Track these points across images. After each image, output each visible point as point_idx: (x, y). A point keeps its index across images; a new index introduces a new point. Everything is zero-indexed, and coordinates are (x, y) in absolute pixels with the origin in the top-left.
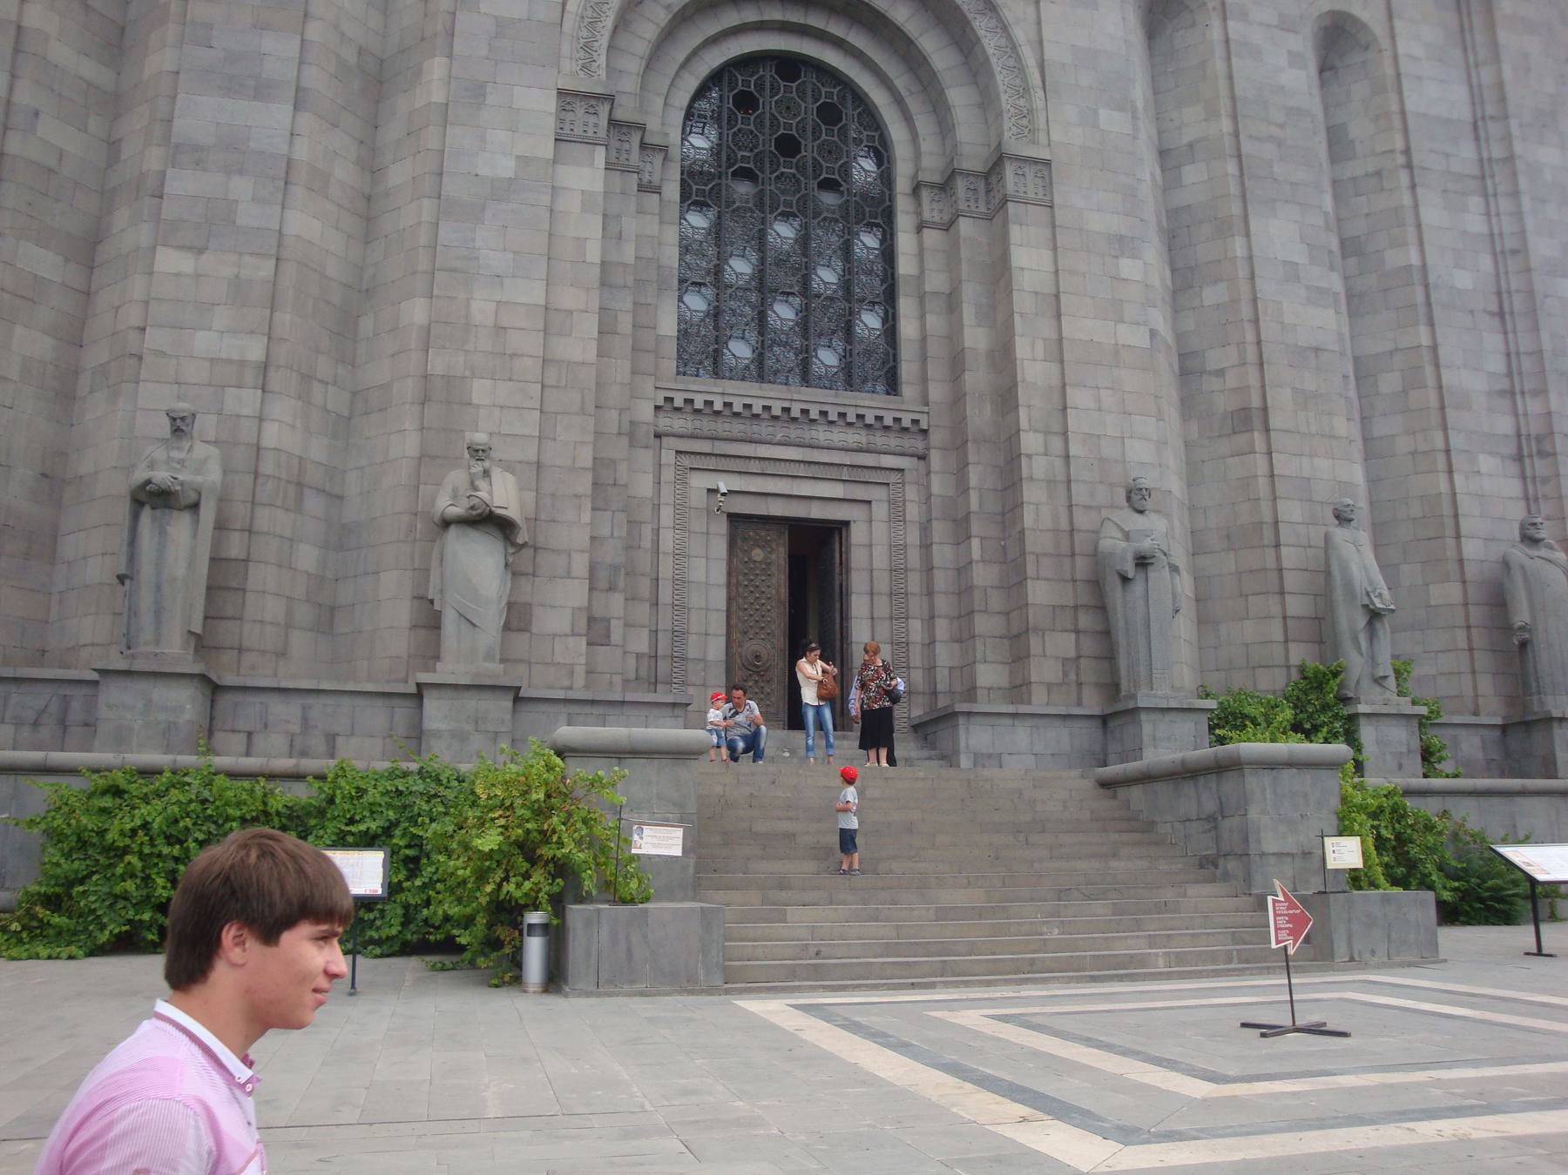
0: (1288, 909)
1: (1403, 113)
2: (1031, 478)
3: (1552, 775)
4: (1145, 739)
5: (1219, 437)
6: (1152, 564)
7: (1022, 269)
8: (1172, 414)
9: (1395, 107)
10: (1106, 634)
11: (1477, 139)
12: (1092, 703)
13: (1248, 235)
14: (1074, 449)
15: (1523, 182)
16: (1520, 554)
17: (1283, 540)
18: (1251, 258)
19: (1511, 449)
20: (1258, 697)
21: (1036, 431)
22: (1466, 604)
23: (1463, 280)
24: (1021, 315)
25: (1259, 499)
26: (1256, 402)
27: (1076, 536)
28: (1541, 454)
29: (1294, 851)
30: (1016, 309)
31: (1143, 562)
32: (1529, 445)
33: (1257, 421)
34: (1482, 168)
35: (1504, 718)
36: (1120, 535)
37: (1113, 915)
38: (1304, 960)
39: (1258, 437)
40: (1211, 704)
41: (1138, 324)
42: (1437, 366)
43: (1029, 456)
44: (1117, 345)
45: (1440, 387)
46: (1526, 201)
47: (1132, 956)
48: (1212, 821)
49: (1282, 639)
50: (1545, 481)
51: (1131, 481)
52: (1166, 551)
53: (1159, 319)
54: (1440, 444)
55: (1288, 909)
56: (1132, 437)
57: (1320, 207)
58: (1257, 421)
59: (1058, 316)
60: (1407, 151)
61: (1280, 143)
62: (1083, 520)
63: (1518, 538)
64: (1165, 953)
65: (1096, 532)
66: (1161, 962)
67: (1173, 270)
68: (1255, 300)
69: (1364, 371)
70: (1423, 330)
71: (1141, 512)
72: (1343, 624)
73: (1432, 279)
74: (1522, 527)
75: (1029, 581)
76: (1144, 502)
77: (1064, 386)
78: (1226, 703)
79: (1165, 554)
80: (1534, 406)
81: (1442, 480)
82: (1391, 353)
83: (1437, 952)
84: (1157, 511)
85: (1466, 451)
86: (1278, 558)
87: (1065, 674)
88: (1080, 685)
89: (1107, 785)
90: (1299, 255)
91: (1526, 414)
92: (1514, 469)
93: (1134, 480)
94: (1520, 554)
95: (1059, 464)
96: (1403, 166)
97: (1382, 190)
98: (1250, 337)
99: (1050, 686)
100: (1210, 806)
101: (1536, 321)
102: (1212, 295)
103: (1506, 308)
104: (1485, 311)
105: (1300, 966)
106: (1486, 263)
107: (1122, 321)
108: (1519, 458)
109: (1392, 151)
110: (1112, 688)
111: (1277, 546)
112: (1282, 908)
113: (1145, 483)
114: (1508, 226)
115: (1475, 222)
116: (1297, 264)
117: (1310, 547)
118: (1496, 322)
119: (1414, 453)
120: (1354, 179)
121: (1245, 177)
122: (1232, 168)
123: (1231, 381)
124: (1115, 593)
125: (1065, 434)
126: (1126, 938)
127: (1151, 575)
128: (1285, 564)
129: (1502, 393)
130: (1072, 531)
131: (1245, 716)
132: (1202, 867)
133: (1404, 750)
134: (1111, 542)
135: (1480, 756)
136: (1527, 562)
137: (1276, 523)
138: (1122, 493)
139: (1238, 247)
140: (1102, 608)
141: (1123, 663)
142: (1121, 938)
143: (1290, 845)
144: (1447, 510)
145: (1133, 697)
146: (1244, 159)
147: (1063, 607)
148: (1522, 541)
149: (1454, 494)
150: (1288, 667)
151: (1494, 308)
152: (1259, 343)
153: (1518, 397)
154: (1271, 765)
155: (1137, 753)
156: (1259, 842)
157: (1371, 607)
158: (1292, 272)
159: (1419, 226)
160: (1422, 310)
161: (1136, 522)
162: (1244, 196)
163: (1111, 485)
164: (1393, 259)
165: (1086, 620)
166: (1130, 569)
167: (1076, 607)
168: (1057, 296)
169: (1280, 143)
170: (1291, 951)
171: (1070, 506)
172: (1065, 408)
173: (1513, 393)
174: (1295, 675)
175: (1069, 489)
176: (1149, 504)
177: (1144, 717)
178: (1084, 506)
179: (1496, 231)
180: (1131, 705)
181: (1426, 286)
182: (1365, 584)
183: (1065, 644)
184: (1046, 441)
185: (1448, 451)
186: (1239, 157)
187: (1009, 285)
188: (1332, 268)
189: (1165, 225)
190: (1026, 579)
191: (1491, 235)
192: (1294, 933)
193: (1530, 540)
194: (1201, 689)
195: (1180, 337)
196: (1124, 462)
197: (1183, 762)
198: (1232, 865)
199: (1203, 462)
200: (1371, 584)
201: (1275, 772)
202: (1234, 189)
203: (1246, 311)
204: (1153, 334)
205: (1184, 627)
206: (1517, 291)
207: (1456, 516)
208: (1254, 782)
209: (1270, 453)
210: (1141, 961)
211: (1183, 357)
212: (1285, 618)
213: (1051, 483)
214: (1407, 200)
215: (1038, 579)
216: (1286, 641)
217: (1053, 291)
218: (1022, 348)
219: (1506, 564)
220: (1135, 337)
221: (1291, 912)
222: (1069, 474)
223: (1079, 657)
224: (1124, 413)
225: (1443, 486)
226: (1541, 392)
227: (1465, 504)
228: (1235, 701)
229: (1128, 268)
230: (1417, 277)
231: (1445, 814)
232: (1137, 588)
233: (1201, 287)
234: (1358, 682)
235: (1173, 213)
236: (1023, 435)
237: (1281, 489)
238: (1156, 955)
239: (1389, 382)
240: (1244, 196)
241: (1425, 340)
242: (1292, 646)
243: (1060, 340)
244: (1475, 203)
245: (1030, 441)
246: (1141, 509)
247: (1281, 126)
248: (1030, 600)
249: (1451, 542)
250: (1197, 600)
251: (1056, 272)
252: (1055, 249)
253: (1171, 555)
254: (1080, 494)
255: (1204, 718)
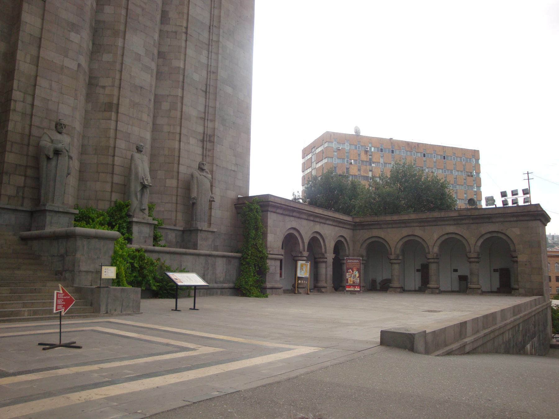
0: (64, 296)
1: (188, 14)
2: (15, 110)
3: (196, 248)
4: (47, 222)
5: (99, 111)
6: (61, 154)
7: (26, 23)
8: (82, 98)
9: (186, 11)
10: (38, 179)
11: (209, 32)
12: (28, 206)
13: (124, 39)
14: (36, 103)
15: (220, 51)
16: (197, 173)
17: (116, 154)
18: (124, 48)
19: (201, 137)
20: (97, 211)
21: (20, 91)
22: (177, 188)
23: (196, 77)
24: (22, 42)
25: (110, 137)
26: (115, 101)
27: (31, 137)
28: (210, 141)
29: (93, 271)
30: (20, 38)
31: (57, 152)
32: (207, 138)
33: (114, 109)
34: (209, 42)
35: (184, 228)
36: (49, 140)
37: (10, 293)
38: (89, 313)
39: (113, 115)
40: (77, 212)
41: (73, 60)
42: (182, 104)
43: (15, 101)
44: (63, 65)
45: (182, 111)
46: (220, 57)
47: (13, 312)
48: (62, 257)
49: (110, 190)
50: (209, 150)
51: (58, 120)
52: (68, 149)
53: (83, 61)
54: (178, 131)
55: (64, 296)
56: (62, 103)
57: (153, 37)
58: (114, 109)
59: (39, 47)
60: (187, 28)
61: (143, 9)
62: (35, 132)
63: (198, 168)
64: (28, 310)
65: (40, 137)
66: (26, 314)
67: (93, 44)
68: (122, 64)
69: (158, 100)
70: (180, 90)
71: (60, 133)
72: (133, 189)
73: (186, 74)
74: (199, 164)
75: (7, 153)
76: (62, 129)
77: (36, 76)
78: (84, 212)
79: (67, 151)
80: (210, 125)
81: (177, 143)
82: (168, 96)
83: (140, 310)
84: (68, 134)
85: (186, 135)
86: (113, 161)
87: (17, 192)
88: (23, 198)
89: (24, 239)
90: (142, 52)
91: (207, 127)
92: (200, 144)
93: (59, 120)
94: (197, 173)
95: (29, 108)
96: (184, 33)
97: (176, 38)
98: (118, 77)
99: (10, 197)
100: (62, 251)
101: (216, 97)
102: (106, 57)
103: (208, 90)
104: (201, 89)
105: (85, 315)
106: (204, 73)
107: (66, 56)
108: (203, 141)
109: (182, 26)
110: (37, 200)
111: (114, 156)
112: (61, 296)
113: (65, 121)
114: (213, 64)
115: (204, 60)
116: (140, 55)
117: (126, 158)
118: (204, 94)
119: (169, 132)
120: (167, 32)
121: (128, 17)
122: (123, 12)
123: (107, 91)
124: (44, 163)
125: (34, 95)
126: (13, 304)
127: (60, 158)
128: (116, 163)
129: (201, 118)
130: (30, 136)
131: (90, 218)
132: (56, 275)
133: (147, 235)
134: (45, 142)
135: (174, 240)
136: (199, 176)
137: (115, 147)
138: (54, 124)
139: (120, 43)
140: (37, 168)
141: (43, 191)
142: (10, 304)
143: (91, 268)
144: (176, 154)
145: (45, 205)
146: (129, 11)
147: (21, 165)
148: (199, 169)
149: (180, 149)
150: (111, 201)
151: (204, 89)
152: (121, 80)
153: (206, 120)
154: (88, 237)
155: (43, 227)
156: (79, 266)
157: (143, 183)
158: (138, 58)
159: (185, 54)
160: (181, 84)
161: (59, 137)
162: (126, 24)
163: (50, 120)
164: (175, 63)
165: (30, 172)
166: (51, 155)
167: (26, 167)
168: (40, 39)
169: (143, 9)
170: (63, 314)
171: (31, 125)
172: (35, 85)
173: (205, 119)
174: (113, 204)
175: (31, 118)
176: (64, 130)
177: (48, 214)
178: (37, 126)
179: (209, 64)
180: (43, 208)
181: (184, 76)
182: (143, 175)
183: (19, 180)
184: (24, 97)
185: (180, 134)
186: (127, 9)
187: (19, 27)
188: (153, 60)
189: (93, 25)
190: (5, 151)
191: (208, 65)
192: (66, 306)
193: (201, 169)
194: (76, 206)
195: (91, 70)
196: (57, 112)
197: (54, 233)
198: (67, 275)
199: (91, 119)
200: (144, 176)
201: (89, 240)
202: (123, 20)
203: (118, 67)
204: (79, 65)
205: (72, 181)
206: (212, 86)
207: (179, 157)
208: (79, 243)
209: (117, 121)
210: (17, 313)
211: (91, 78)
212: (112, 183)
213: (24, 114)
214: (183, 44)
215: (11, 152)
216: (112, 192)
217: (39, 36)
218: (20, 55)
219: (192, 176)
220: (73, 66)
221: (65, 297)
222: (32, 112)
223: (24, 187)
224: (61, 93)
225: (177, 146)
226: (213, 121)
227: (183, 153)
228: (87, 211)
229: (74, 36)
230: (181, 72)
231: (158, 259)
232: (53, 163)
233: (103, 53)
234: (135, 210)
235: (98, 22)
236: (14, 92)
237: (119, 135)
238: (24, 311)
239: (165, 106)
240: (126, 24)
241: (180, 94)
242: (113, 194)
243: (38, 57)
244: (205, 52)
245: (17, 95)
246: (60, 132)
247: (145, 3)
248: (6, 160)
249: (176, 165)
250: (80, 171)
251: (42, 29)
252: (43, 19)
253: (69, 152)
254: (36, 121)
255: (73, 217)
